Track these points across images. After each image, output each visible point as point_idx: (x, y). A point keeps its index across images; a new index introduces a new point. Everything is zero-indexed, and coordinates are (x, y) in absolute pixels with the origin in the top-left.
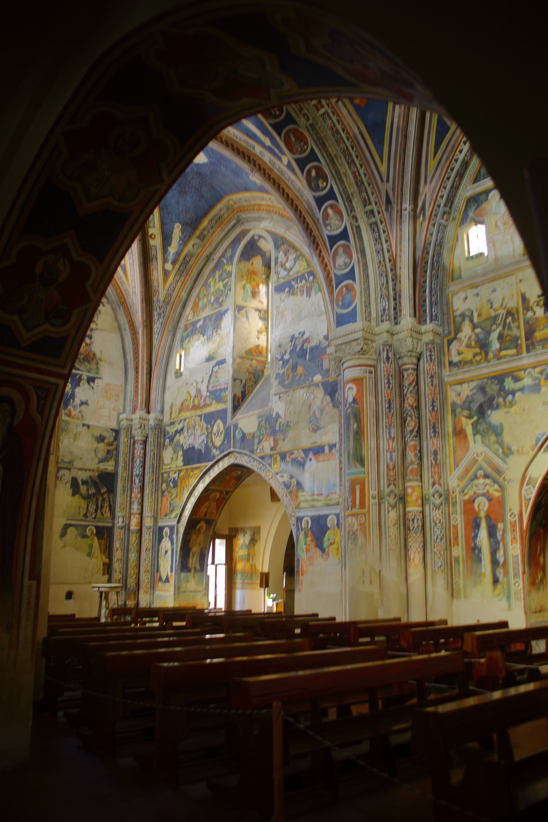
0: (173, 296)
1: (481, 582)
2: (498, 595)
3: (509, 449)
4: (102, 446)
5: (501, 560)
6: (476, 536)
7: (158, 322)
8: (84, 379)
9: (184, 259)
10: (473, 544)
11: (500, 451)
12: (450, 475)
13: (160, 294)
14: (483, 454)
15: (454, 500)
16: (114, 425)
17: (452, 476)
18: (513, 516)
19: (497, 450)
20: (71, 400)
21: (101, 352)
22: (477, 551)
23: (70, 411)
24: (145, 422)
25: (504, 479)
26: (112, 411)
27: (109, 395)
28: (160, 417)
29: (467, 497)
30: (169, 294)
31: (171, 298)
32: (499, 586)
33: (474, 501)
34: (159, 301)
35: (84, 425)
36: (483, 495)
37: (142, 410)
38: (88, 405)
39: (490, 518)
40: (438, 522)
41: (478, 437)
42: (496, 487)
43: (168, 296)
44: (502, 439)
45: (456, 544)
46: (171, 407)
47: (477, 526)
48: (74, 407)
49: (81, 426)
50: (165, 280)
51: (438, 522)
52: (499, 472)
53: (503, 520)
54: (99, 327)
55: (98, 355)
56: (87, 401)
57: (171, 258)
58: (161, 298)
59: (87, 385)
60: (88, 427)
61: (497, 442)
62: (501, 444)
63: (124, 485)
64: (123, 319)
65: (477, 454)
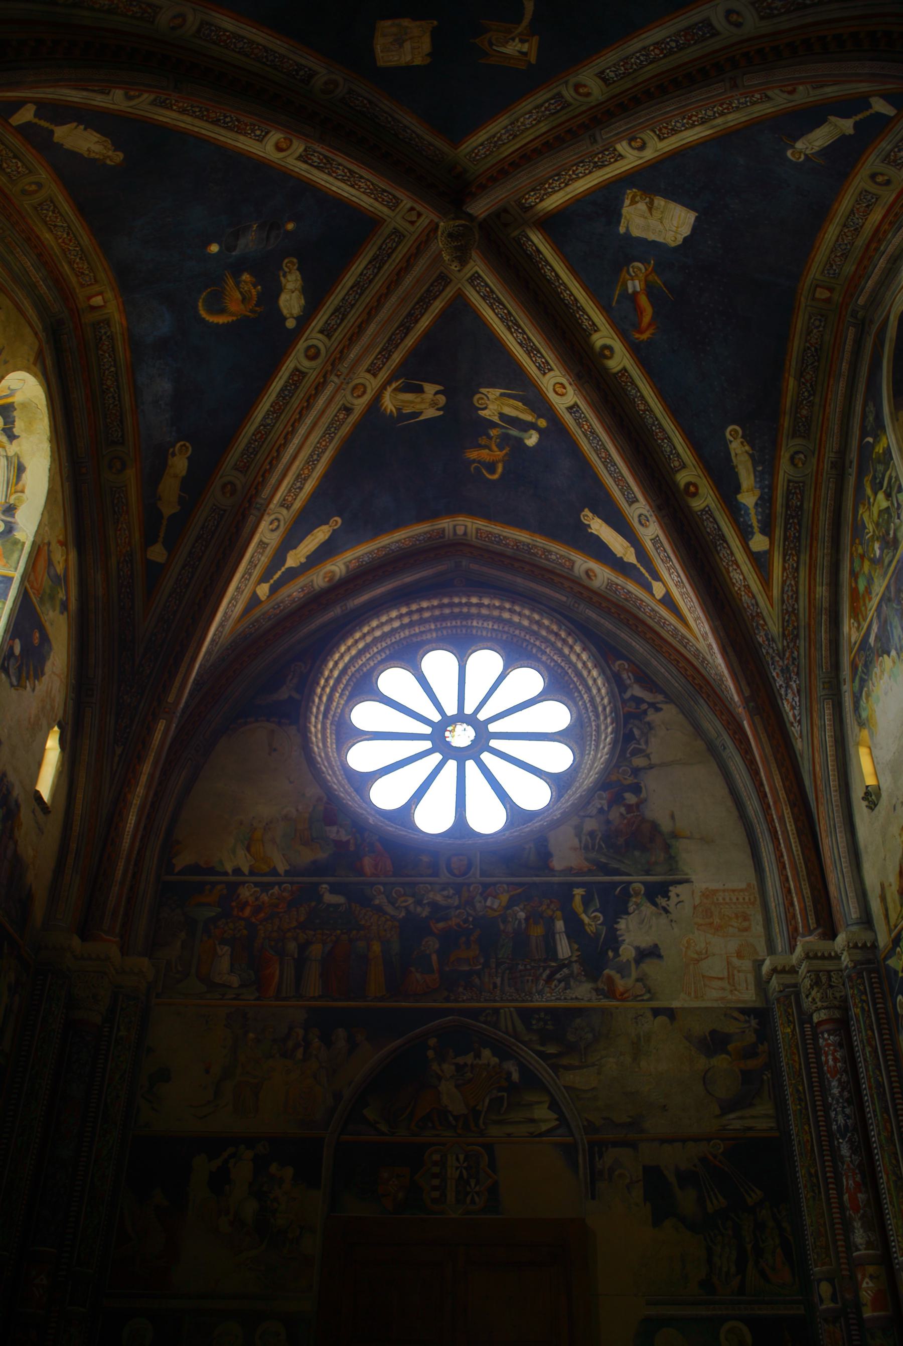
0: (801, 609)
4: (721, 1062)
7: (789, 691)
8: (637, 894)
9: (788, 507)
13: (770, 623)
16: (748, 995)
20: (611, 954)
21: (672, 817)
23: (610, 980)
24: (829, 965)
26: (735, 961)
27: (717, 920)
28: (865, 937)
30: (790, 609)
31: (797, 616)
34: (773, 640)
35: (656, 1012)
37: (810, 932)
38: (660, 956)
43: (789, 614)
46: (883, 898)
48: (623, 970)
49: (649, 1014)
50: (766, 582)
54: (655, 760)
55: (666, 826)
56: (656, 946)
57: (754, 521)
58: (775, 628)
59: (648, 909)
60: (671, 1014)
63: (813, 1171)
64: (712, 725)
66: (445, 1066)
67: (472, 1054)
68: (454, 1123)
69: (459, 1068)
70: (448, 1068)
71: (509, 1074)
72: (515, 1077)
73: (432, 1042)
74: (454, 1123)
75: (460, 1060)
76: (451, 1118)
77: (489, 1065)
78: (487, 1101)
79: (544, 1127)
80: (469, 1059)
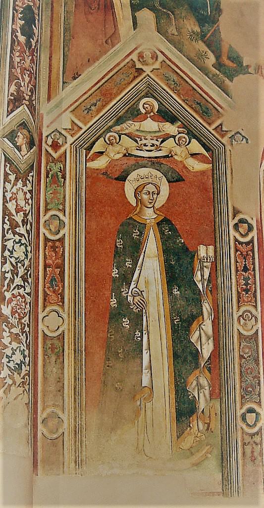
1: (137, 413)
2: (191, 452)
3: (236, 59)
5: (207, 350)
6: (126, 278)
10: (113, 302)
11: (212, 59)
12: (49, 99)
14: (161, 58)
15: (55, 168)
17: (53, 102)
18: (243, 228)
19: (201, 56)
22: (126, 322)
25: (219, 128)
29: (100, 163)
32: (197, 425)
33: (123, 178)
36: (155, 163)
39: (173, 229)
40: (19, 218)
41: (146, 16)
42: (196, 147)
44: (217, 32)
45: (53, 297)
47: (135, 249)
51: (19, 218)
52: (206, 110)
53: (213, 239)
61: (203, 37)
62: (213, 45)
65: (141, 56)
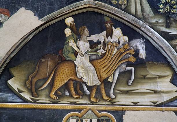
66: (81, 43)
67: (105, 32)
68: (88, 92)
69: (93, 45)
70: (84, 46)
71: (137, 53)
72: (143, 54)
73: (69, 21)
74: (88, 92)
75: (94, 38)
76: (86, 88)
77: (119, 43)
78: (117, 74)
79: (166, 98)
80: (101, 37)
